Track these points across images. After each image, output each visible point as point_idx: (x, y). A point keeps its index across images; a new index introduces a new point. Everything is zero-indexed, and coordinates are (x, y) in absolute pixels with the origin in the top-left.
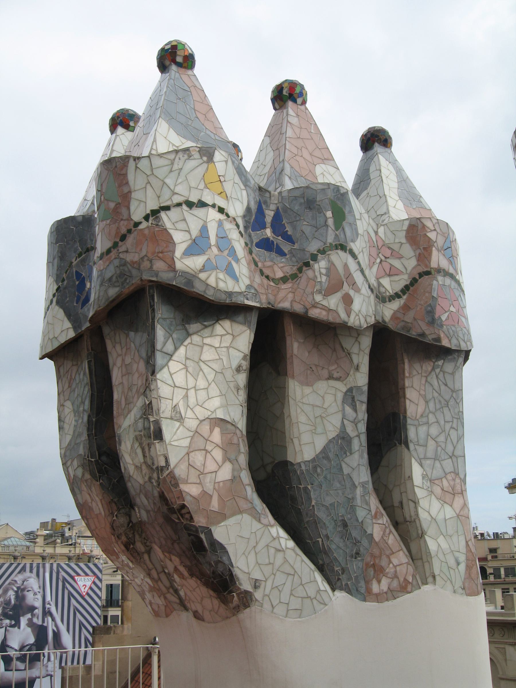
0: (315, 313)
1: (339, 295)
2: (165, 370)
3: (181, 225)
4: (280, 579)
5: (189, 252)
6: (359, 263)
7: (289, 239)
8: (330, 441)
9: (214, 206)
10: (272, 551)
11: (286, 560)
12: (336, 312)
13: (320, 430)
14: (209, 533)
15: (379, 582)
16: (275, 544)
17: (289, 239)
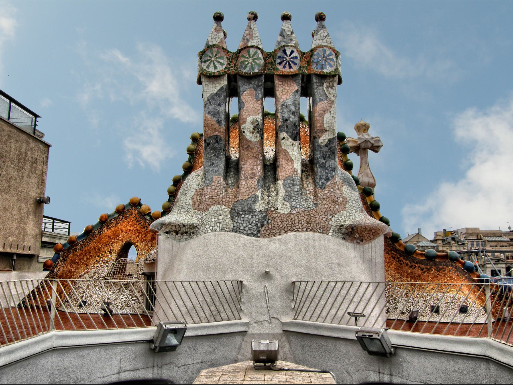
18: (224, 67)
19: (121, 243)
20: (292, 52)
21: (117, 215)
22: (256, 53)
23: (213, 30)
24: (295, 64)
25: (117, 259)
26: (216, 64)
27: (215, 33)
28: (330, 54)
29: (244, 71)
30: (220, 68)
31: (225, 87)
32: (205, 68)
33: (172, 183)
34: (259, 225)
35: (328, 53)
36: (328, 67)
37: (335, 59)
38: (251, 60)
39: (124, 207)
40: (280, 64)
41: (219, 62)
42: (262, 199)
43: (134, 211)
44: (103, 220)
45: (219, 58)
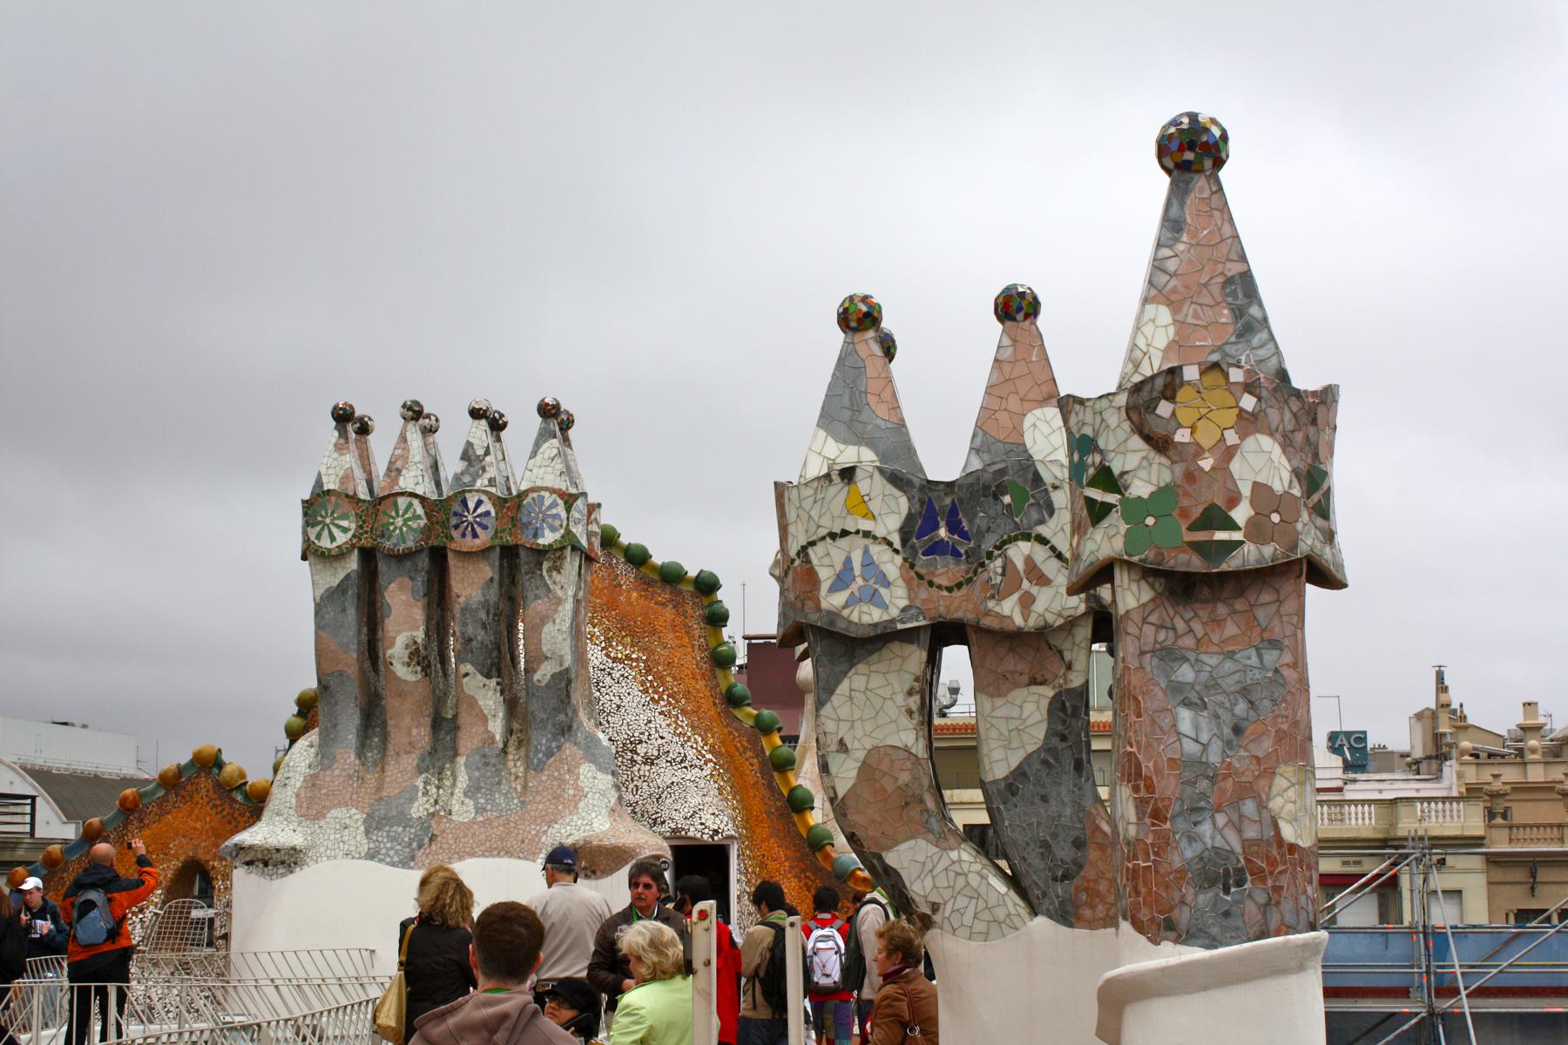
0: (987, 622)
1: (1016, 596)
2: (828, 705)
3: (826, 561)
4: (962, 902)
5: (834, 589)
6: (1053, 549)
7: (964, 535)
8: (1030, 756)
9: (857, 532)
10: (952, 875)
11: (968, 884)
12: (1010, 618)
13: (1015, 744)
14: (880, 858)
15: (1093, 907)
16: (956, 867)
17: (964, 535)
18: (350, 535)
19: (175, 864)
20: (479, 503)
21: (161, 793)
22: (410, 505)
23: (331, 447)
24: (485, 527)
25: (164, 903)
26: (335, 531)
27: (336, 455)
28: (554, 505)
29: (388, 544)
30: (342, 538)
31: (354, 576)
32: (313, 538)
33: (295, 709)
34: (415, 845)
35: (547, 503)
36: (547, 532)
37: (564, 514)
38: (399, 522)
39: (180, 771)
40: (456, 527)
41: (339, 527)
42: (426, 793)
43: (204, 783)
44: (128, 805)
45: (340, 518)
